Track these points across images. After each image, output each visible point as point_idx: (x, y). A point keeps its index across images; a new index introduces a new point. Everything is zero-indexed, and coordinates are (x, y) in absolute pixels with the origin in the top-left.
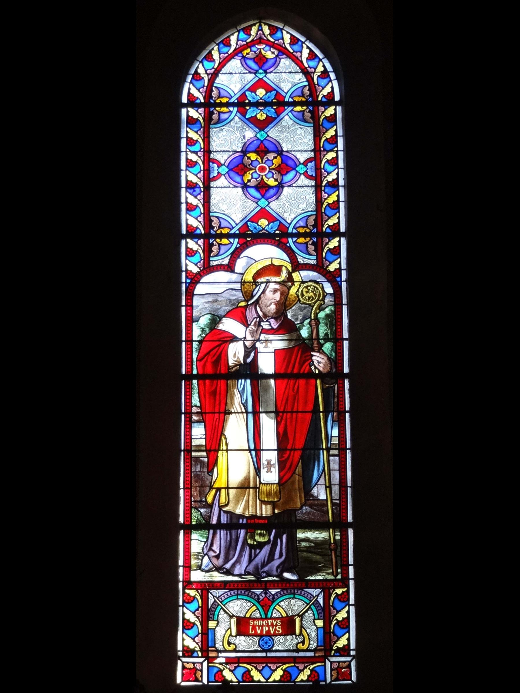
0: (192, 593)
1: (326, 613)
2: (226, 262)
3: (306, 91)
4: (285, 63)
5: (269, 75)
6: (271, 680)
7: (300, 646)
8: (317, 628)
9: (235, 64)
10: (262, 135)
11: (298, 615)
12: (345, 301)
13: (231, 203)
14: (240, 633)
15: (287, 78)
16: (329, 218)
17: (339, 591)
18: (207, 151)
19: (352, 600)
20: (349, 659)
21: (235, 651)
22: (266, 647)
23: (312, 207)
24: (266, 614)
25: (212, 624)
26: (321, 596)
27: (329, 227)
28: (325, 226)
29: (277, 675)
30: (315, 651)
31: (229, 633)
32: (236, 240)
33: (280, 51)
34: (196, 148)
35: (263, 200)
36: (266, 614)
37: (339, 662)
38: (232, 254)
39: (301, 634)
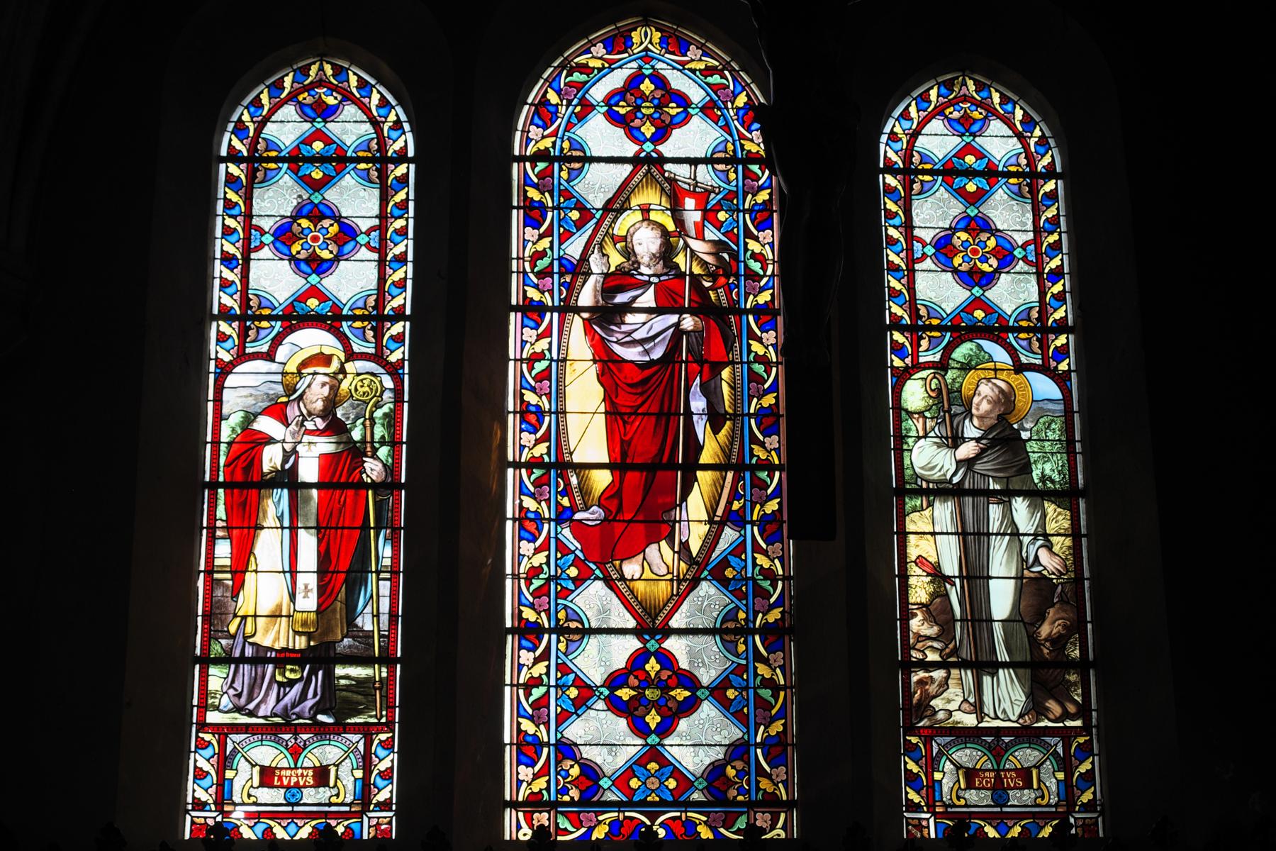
0: (914, 740)
1: (1065, 764)
2: (937, 358)
3: (1023, 161)
4: (996, 126)
5: (977, 139)
6: (1009, 836)
7: (1039, 801)
8: (1058, 781)
9: (936, 125)
10: (972, 212)
11: (1035, 766)
12: (1076, 408)
13: (940, 291)
14: (970, 786)
15: (999, 144)
16: (1055, 310)
17: (1081, 740)
18: (908, 226)
19: (1096, 751)
20: (1095, 815)
21: (966, 806)
22: (1001, 802)
23: (1035, 297)
24: (998, 765)
25: (937, 776)
26: (1060, 745)
27: (1055, 321)
28: (1051, 320)
29: (1016, 831)
30: (1056, 805)
31: (957, 786)
32: (948, 334)
33: (988, 111)
34: (897, 221)
35: (977, 288)
36: (998, 765)
37: (1084, 819)
38: (944, 348)
39: (1039, 788)
